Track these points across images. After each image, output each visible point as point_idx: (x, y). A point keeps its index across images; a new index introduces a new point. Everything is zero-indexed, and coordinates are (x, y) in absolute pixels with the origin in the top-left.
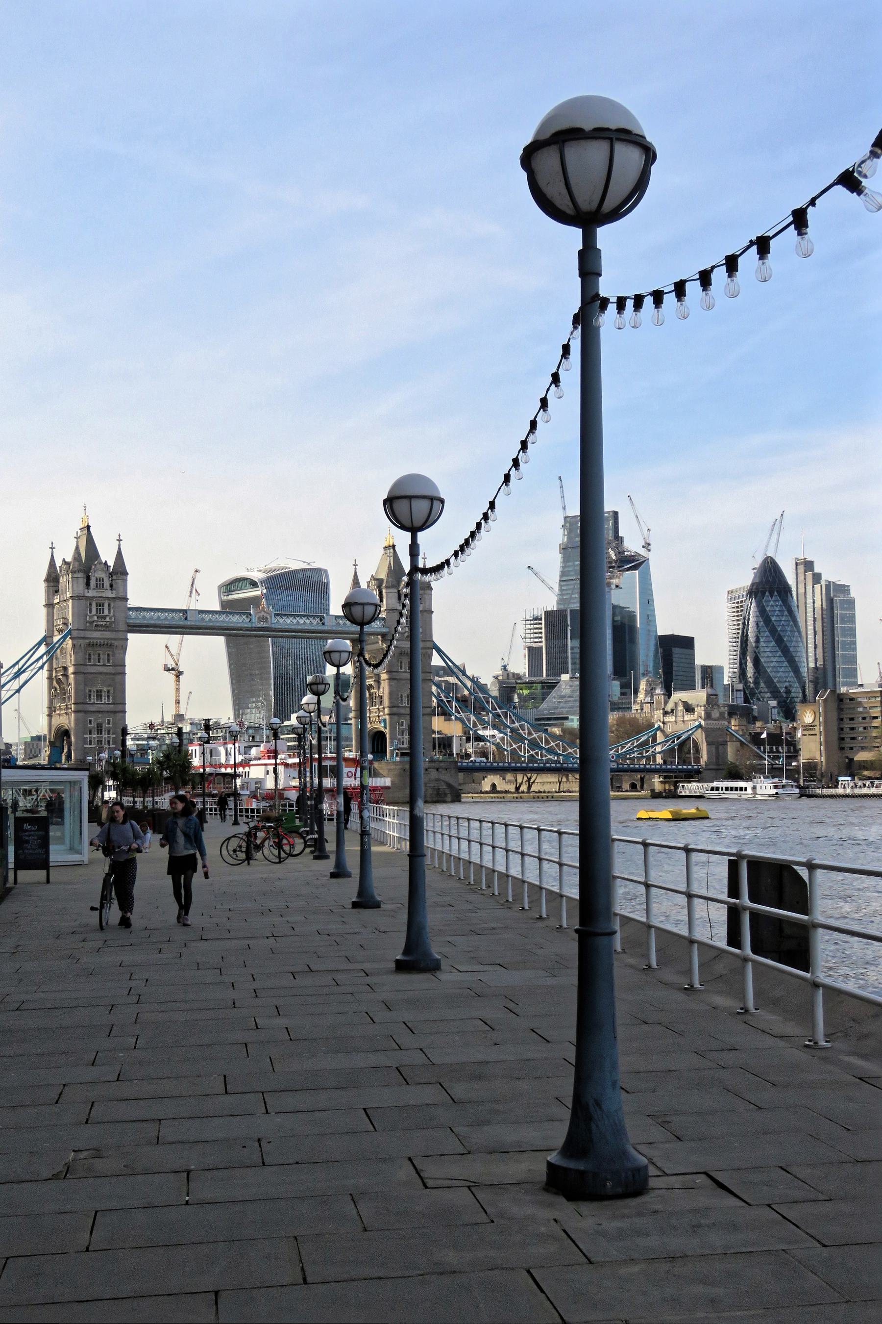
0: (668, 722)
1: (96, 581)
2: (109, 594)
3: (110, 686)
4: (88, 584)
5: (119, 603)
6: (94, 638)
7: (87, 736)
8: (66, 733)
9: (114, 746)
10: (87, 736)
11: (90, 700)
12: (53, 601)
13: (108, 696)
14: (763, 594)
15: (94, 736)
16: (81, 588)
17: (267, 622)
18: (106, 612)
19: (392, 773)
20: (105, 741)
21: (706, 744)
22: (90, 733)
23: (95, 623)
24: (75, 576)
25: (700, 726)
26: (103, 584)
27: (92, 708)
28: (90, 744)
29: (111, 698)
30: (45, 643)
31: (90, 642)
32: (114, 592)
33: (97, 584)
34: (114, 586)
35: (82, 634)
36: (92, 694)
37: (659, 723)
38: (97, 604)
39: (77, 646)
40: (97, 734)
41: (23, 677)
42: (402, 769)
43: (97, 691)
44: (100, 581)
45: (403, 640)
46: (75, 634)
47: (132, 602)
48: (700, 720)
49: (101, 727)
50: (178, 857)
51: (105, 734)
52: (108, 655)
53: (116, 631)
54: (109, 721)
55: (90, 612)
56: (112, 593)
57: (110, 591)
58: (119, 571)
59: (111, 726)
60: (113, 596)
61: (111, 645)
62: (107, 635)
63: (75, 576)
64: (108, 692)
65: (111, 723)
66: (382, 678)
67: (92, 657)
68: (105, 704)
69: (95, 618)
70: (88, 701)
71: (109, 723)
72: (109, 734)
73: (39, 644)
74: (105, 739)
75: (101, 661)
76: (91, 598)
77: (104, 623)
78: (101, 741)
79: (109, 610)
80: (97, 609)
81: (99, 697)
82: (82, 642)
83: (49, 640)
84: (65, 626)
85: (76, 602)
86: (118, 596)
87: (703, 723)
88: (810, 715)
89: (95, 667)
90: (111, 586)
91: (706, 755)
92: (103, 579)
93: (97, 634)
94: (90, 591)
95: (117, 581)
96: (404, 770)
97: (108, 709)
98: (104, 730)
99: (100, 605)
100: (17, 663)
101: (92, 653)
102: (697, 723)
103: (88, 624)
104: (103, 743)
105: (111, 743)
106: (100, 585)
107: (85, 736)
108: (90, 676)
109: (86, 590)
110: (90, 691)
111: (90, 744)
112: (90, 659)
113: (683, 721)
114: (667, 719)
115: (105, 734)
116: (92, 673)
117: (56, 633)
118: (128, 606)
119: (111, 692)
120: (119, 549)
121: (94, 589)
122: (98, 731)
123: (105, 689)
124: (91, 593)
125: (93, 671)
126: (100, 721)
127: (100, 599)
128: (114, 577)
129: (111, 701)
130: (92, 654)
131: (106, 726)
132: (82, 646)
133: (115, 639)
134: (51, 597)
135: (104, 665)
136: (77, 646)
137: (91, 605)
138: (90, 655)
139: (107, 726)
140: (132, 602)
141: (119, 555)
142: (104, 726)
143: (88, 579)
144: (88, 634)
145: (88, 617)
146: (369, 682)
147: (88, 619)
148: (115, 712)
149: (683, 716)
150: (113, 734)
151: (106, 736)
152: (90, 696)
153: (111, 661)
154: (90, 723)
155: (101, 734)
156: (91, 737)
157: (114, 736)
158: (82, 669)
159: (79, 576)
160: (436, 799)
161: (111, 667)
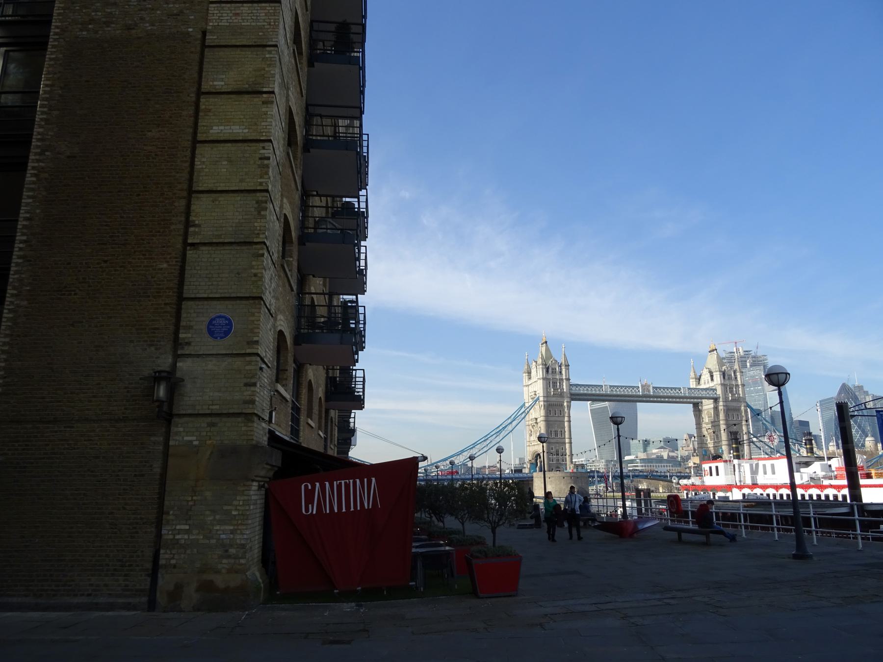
6: (553, 401)
8: (539, 454)
11: (551, 436)
13: (562, 434)
18: (558, 387)
36: (552, 433)
38: (553, 382)
41: (514, 423)
43: (555, 431)
50: (610, 532)
52: (561, 411)
55: (550, 387)
64: (561, 432)
67: (552, 412)
68: (560, 438)
71: (563, 450)
77: (557, 393)
93: (554, 399)
99: (555, 384)
100: (510, 417)
101: (551, 409)
108: (551, 423)
110: (551, 431)
111: (553, 461)
112: (550, 413)
117: (531, 400)
123: (559, 430)
126: (557, 448)
134: (527, 381)
135: (559, 416)
137: (549, 383)
138: (550, 411)
142: (560, 451)
152: (551, 434)
153: (562, 414)
154: (552, 449)
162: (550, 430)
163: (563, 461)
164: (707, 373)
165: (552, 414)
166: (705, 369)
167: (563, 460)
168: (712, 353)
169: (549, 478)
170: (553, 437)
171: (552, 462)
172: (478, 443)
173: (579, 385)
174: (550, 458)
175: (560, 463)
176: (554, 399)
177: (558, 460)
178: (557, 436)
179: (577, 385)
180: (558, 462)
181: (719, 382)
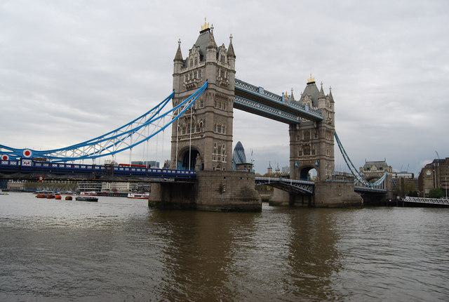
2: (226, 66)
4: (217, 58)
5: (232, 73)
8: (195, 152)
18: (225, 77)
27: (216, 136)
47: (238, 76)
58: (231, 55)
62: (226, 92)
73: (169, 98)
76: (219, 67)
81: (219, 130)
82: (214, 92)
93: (220, 90)
106: (222, 60)
124: (219, 64)
140: (238, 76)
141: (231, 47)
143: (218, 54)
144: (217, 88)
172: (106, 137)
176: (220, 90)
177: (219, 159)
179: (240, 82)
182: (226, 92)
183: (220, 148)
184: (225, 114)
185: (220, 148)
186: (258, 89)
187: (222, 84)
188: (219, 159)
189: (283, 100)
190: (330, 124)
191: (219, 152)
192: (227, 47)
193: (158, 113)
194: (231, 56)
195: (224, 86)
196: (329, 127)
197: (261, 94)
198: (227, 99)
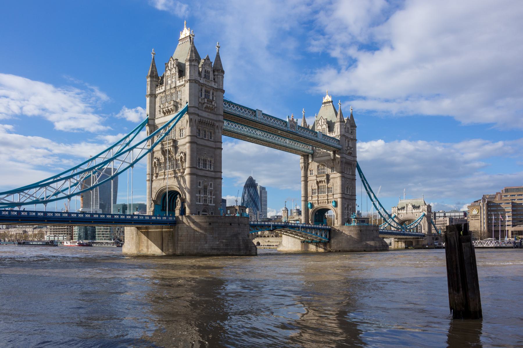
0: (401, 213)
1: (205, 73)
2: (213, 84)
3: (212, 157)
5: (220, 93)
7: (198, 195)
8: (173, 194)
9: (214, 205)
10: (198, 195)
11: (199, 167)
12: (155, 91)
14: (249, 188)
15: (202, 196)
16: (196, 76)
17: (294, 128)
18: (211, 98)
19: (353, 232)
20: (209, 201)
21: (427, 223)
22: (200, 194)
23: (205, 105)
24: (193, 64)
25: (424, 215)
26: (209, 76)
28: (200, 202)
29: (212, 167)
30: (147, 124)
31: (201, 120)
32: (216, 84)
33: (205, 75)
34: (216, 80)
35: (197, 111)
37: (395, 214)
39: (193, 121)
40: (204, 195)
42: (359, 230)
44: (207, 74)
45: (346, 154)
46: (191, 110)
48: (424, 212)
49: (206, 189)
51: (209, 195)
53: (217, 115)
54: (211, 184)
55: (201, 96)
56: (215, 85)
57: (214, 83)
59: (212, 189)
60: (215, 87)
61: (213, 125)
62: (212, 116)
63: (193, 64)
65: (212, 186)
66: (331, 177)
67: (201, 132)
68: (208, 171)
69: (206, 100)
70: (198, 166)
72: (211, 195)
74: (209, 198)
75: (207, 136)
76: (202, 85)
78: (206, 200)
79: (213, 97)
80: (205, 94)
81: (205, 165)
83: (151, 122)
84: (175, 107)
85: (194, 84)
86: (218, 88)
87: (426, 213)
88: (476, 211)
89: (203, 141)
90: (214, 79)
91: (427, 229)
92: (209, 72)
93: (205, 114)
94: (201, 78)
95: (218, 76)
96: (361, 231)
97: (210, 175)
98: (208, 191)
99: (207, 92)
102: (422, 214)
103: (200, 104)
104: (208, 202)
105: (212, 202)
106: (207, 77)
107: (197, 195)
109: (199, 78)
110: (199, 160)
112: (199, 134)
113: (412, 213)
114: (400, 212)
115: (209, 195)
116: (201, 145)
118: (224, 98)
119: (213, 162)
120: (218, 53)
121: (204, 78)
122: (204, 191)
123: (209, 159)
124: (202, 81)
125: (201, 143)
127: (208, 87)
128: (216, 73)
129: (212, 169)
130: (201, 130)
131: (209, 188)
132: (197, 121)
133: (216, 121)
135: (208, 140)
136: (193, 121)
137: (201, 90)
138: (199, 130)
139: (210, 188)
141: (218, 57)
145: (200, 99)
146: (319, 179)
147: (200, 101)
148: (215, 178)
149: (412, 210)
150: (213, 196)
151: (209, 196)
152: (199, 163)
153: (213, 138)
155: (206, 195)
156: (200, 197)
157: (214, 197)
158: (196, 140)
159: (196, 64)
160: (382, 248)
161: (213, 143)
162: (198, 157)
163: (211, 203)
164: (325, 123)
165: (201, 135)
166: (323, 120)
167: (211, 201)
168: (328, 104)
169: (210, 224)
170: (201, 167)
171: (198, 203)
173: (232, 103)
174: (197, 197)
175: (208, 205)
176: (205, 114)
177: (205, 200)
178: (206, 168)
179: (230, 103)
180: (205, 204)
181: (339, 134)
182: (212, 116)
183: (205, 188)
184: (212, 144)
185: (205, 188)
186: (254, 112)
187: (206, 108)
188: (205, 200)
189: (289, 126)
190: (350, 154)
191: (205, 192)
192: (213, 60)
193: (128, 144)
194: (218, 70)
195: (212, 110)
196: (349, 158)
197: (259, 118)
198: (213, 125)
